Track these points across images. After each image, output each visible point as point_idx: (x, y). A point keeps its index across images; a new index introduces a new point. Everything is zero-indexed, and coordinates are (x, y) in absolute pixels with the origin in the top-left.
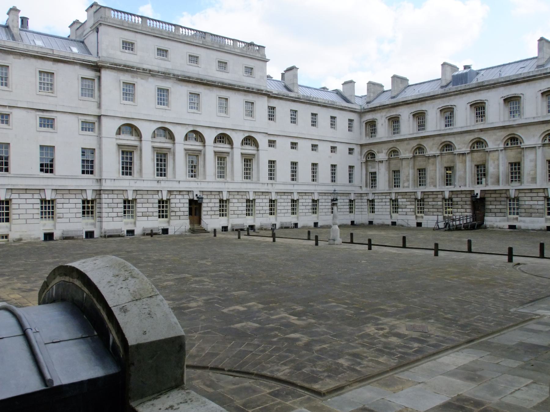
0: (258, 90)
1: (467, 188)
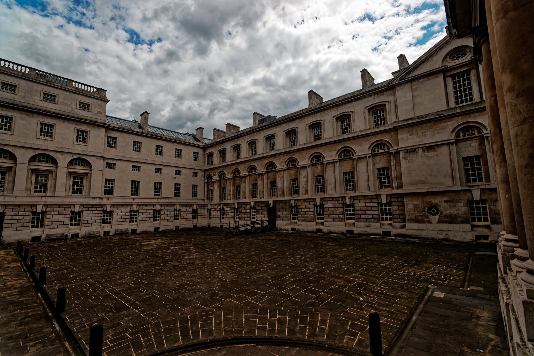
0: (92, 121)
1: (265, 199)
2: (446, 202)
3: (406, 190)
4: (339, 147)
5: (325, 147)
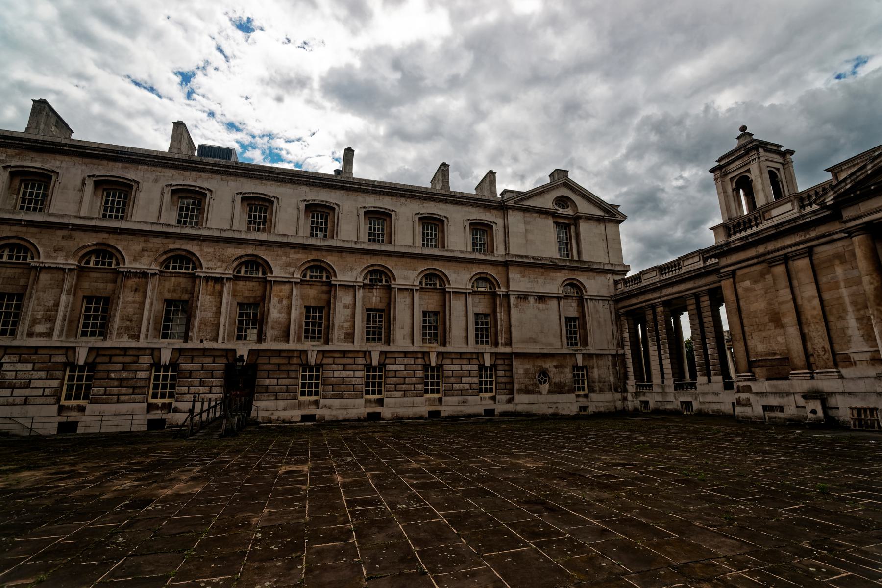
2: (556, 367)
3: (517, 348)
4: (423, 266)
5: (395, 259)
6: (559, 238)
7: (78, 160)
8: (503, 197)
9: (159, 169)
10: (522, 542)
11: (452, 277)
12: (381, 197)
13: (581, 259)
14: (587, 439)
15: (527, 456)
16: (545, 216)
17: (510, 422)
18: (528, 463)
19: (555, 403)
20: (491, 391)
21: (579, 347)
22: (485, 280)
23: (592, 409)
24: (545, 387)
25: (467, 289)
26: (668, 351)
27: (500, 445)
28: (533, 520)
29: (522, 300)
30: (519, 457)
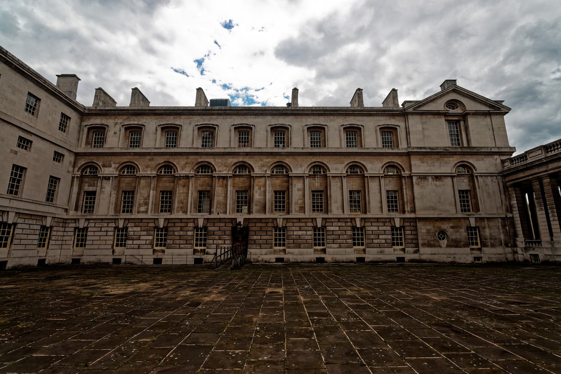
2: (452, 227)
4: (348, 160)
5: (329, 157)
6: (451, 131)
7: (153, 117)
8: (403, 107)
9: (191, 117)
10: (435, 352)
11: (368, 166)
12: (317, 117)
13: (470, 146)
14: (482, 282)
15: (433, 291)
16: (438, 116)
17: (418, 267)
18: (435, 297)
19: (453, 254)
20: (401, 244)
21: (471, 212)
22: (393, 166)
23: (485, 259)
24: (444, 242)
25: (380, 174)
26: (556, 214)
27: (411, 283)
28: (442, 338)
29: (422, 179)
30: (427, 292)
